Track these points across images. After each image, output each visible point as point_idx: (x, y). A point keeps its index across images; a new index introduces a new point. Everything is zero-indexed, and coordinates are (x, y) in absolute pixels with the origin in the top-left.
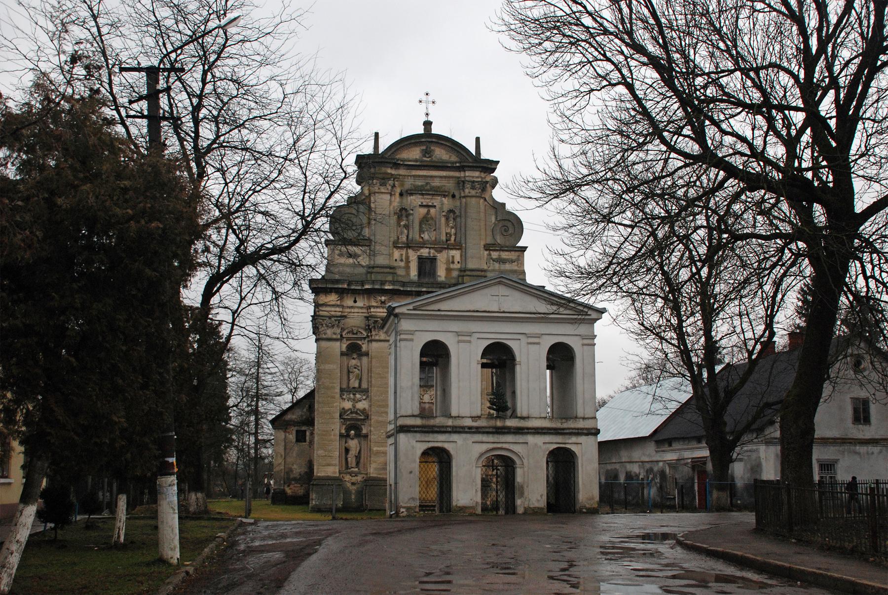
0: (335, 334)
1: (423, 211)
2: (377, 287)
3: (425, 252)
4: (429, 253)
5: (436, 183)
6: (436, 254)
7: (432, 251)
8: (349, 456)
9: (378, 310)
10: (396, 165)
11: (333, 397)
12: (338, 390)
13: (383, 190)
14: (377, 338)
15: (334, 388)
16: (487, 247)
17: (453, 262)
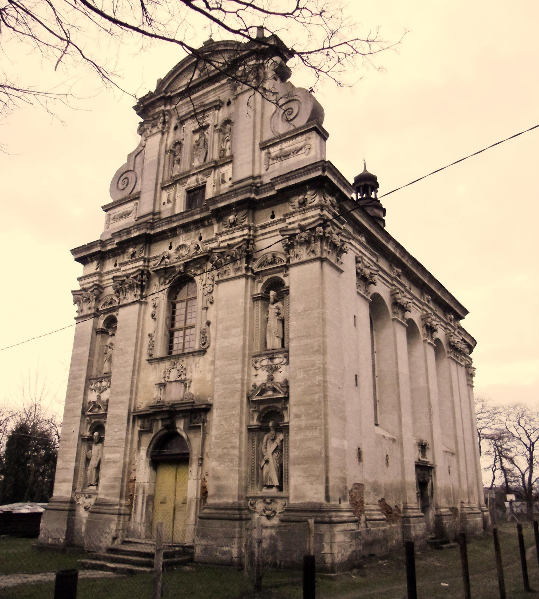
0: (90, 308)
1: (197, 137)
2: (124, 238)
3: (192, 182)
4: (197, 181)
5: (211, 98)
6: (205, 179)
7: (200, 176)
8: (89, 468)
9: (128, 267)
10: (168, 100)
11: (79, 389)
12: (83, 379)
13: (155, 130)
14: (125, 302)
15: (80, 376)
16: (264, 146)
17: (223, 182)
